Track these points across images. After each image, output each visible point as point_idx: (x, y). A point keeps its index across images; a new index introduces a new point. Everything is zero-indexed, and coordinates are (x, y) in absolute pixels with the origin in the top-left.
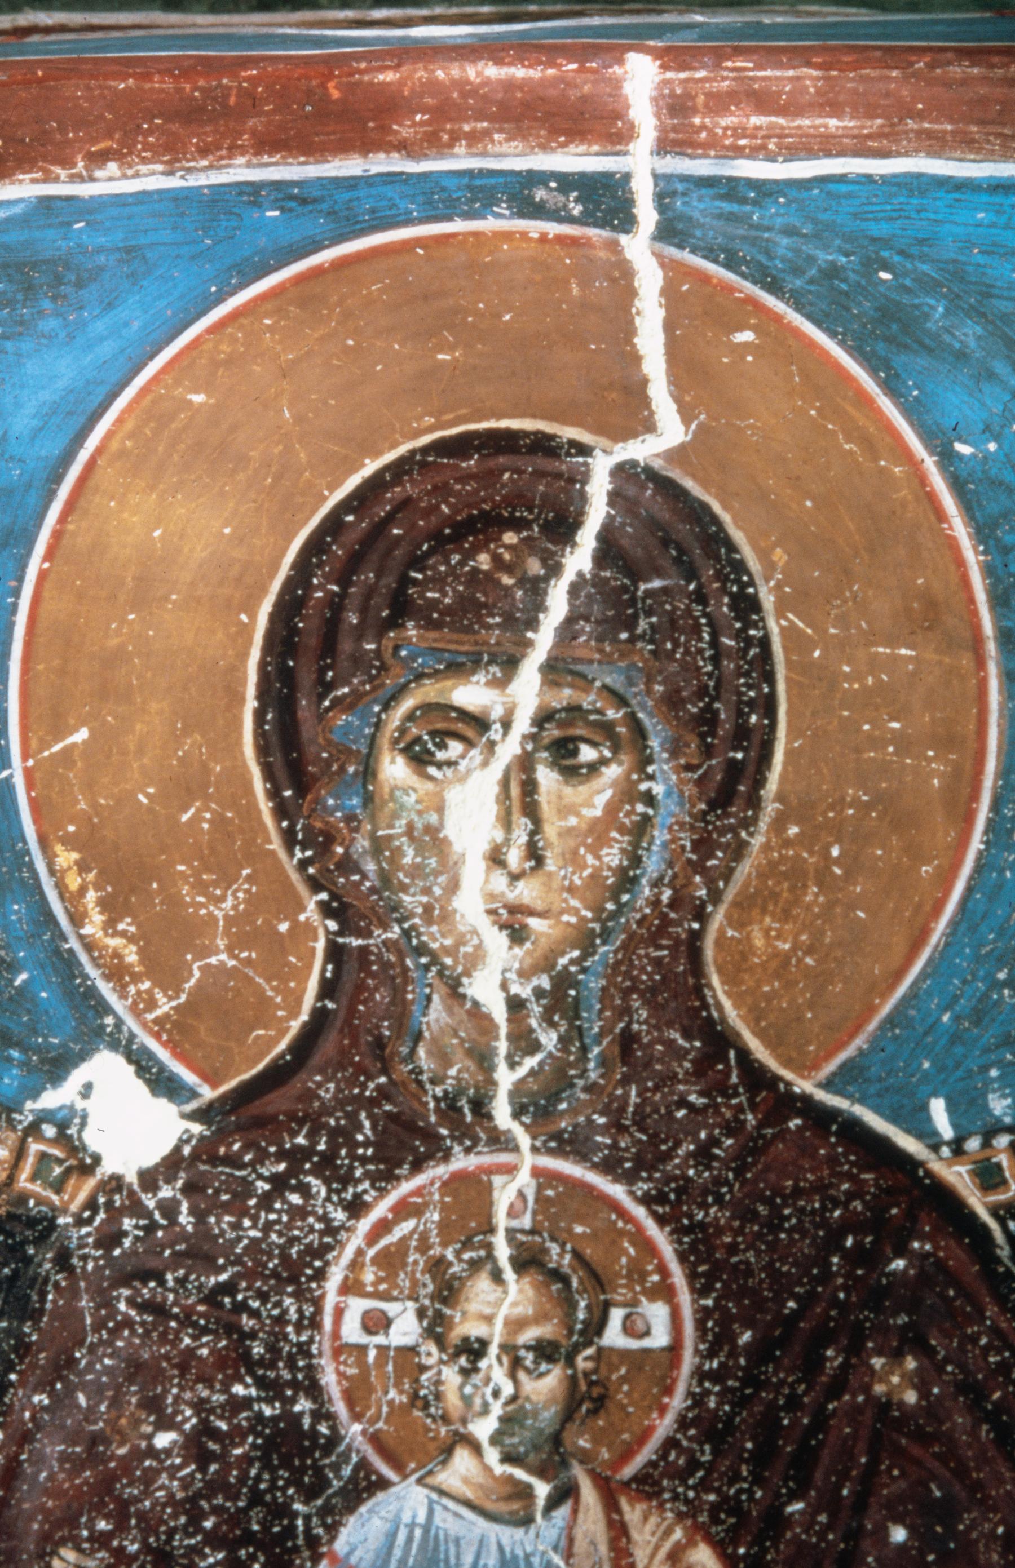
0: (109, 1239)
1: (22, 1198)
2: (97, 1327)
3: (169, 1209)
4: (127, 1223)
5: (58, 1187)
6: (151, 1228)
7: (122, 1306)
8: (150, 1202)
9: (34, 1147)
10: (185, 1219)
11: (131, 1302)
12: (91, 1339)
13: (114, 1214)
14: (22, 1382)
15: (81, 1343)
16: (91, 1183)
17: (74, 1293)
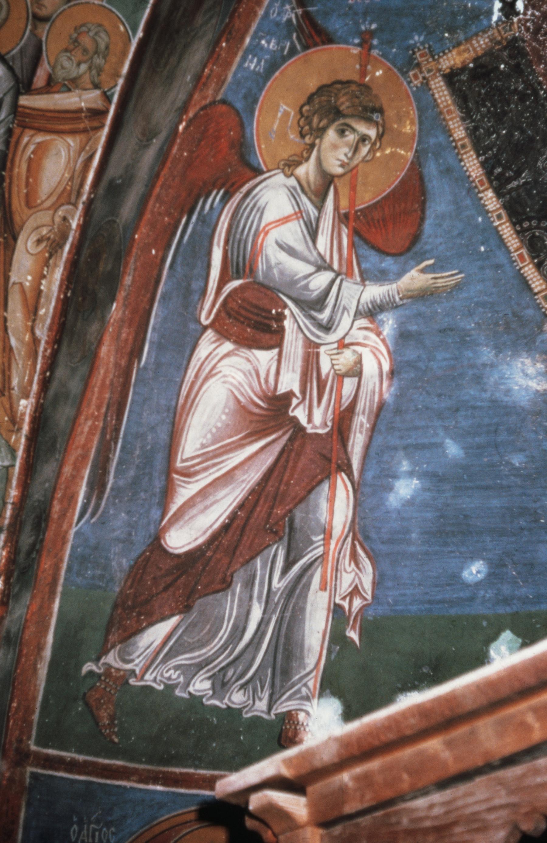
0: (527, 29)
1: (506, 38)
2: (540, 45)
3: (533, 15)
4: (528, 24)
5: (511, 30)
6: (533, 21)
7: (541, 38)
8: (528, 17)
9: (500, 28)
10: (537, 13)
11: (542, 36)
12: (541, 48)
13: (524, 25)
14: (537, 66)
15: (540, 51)
16: (516, 26)
17: (530, 45)
